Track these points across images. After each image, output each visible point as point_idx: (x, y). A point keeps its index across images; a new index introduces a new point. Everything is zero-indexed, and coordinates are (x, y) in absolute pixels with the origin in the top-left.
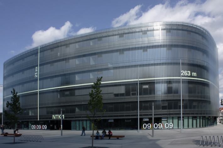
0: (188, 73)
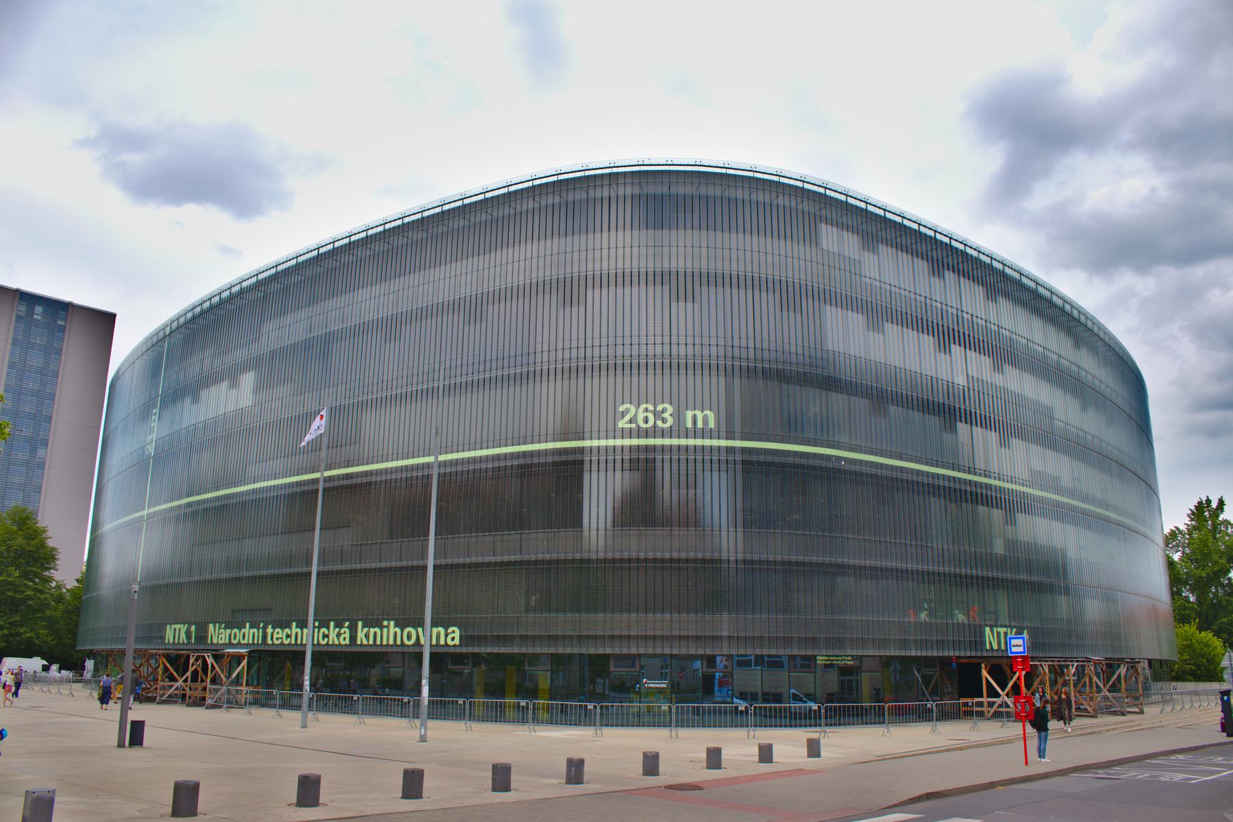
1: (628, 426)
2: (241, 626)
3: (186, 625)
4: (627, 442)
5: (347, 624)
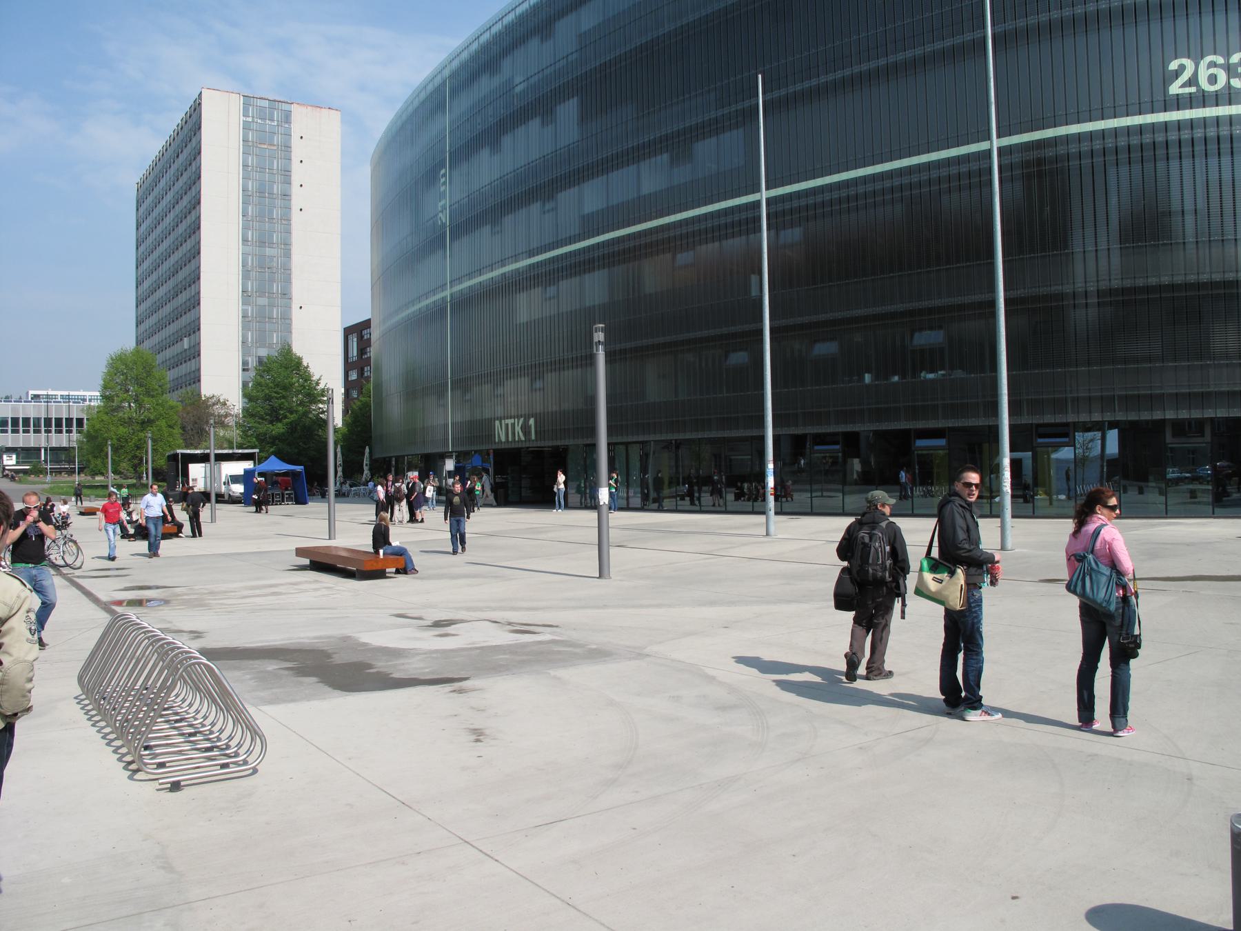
3: (522, 420)
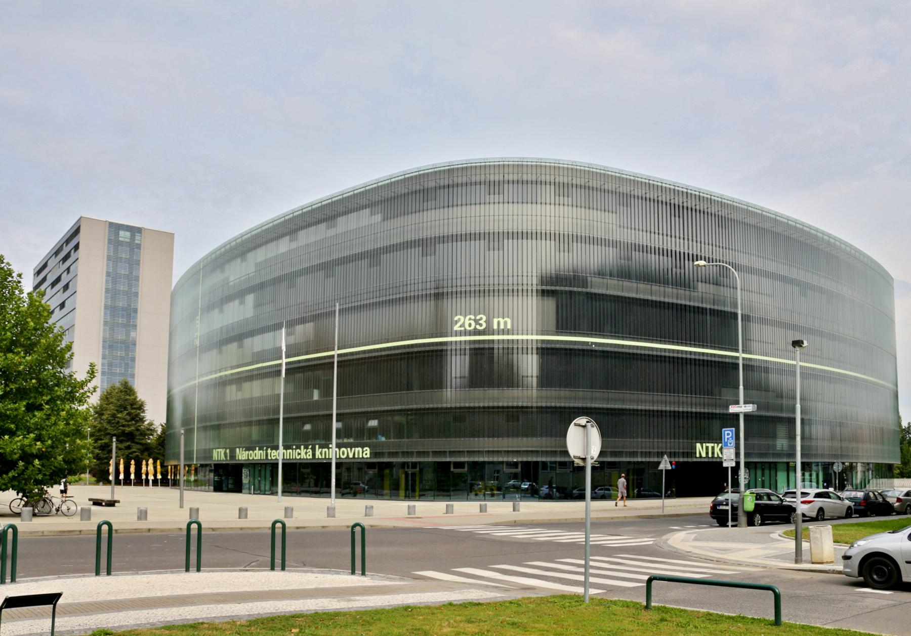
0: (477, 322)
1: (460, 329)
2: (253, 449)
4: (458, 339)
5: (310, 447)
